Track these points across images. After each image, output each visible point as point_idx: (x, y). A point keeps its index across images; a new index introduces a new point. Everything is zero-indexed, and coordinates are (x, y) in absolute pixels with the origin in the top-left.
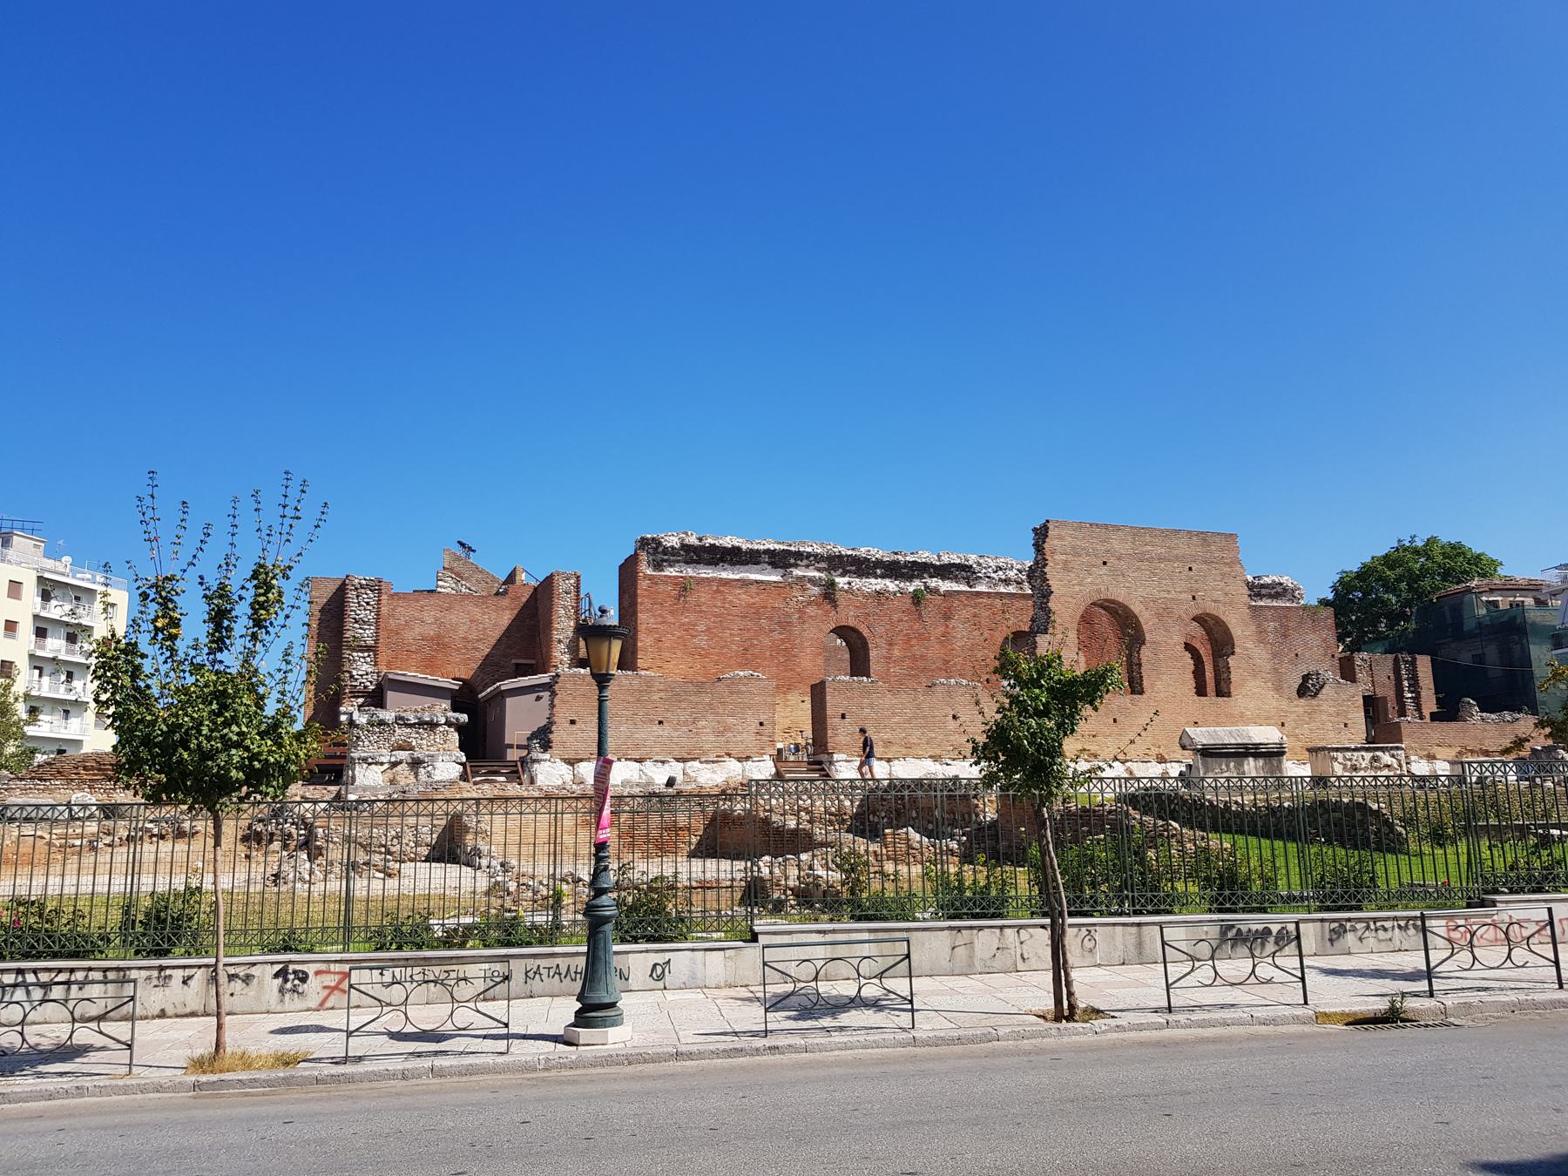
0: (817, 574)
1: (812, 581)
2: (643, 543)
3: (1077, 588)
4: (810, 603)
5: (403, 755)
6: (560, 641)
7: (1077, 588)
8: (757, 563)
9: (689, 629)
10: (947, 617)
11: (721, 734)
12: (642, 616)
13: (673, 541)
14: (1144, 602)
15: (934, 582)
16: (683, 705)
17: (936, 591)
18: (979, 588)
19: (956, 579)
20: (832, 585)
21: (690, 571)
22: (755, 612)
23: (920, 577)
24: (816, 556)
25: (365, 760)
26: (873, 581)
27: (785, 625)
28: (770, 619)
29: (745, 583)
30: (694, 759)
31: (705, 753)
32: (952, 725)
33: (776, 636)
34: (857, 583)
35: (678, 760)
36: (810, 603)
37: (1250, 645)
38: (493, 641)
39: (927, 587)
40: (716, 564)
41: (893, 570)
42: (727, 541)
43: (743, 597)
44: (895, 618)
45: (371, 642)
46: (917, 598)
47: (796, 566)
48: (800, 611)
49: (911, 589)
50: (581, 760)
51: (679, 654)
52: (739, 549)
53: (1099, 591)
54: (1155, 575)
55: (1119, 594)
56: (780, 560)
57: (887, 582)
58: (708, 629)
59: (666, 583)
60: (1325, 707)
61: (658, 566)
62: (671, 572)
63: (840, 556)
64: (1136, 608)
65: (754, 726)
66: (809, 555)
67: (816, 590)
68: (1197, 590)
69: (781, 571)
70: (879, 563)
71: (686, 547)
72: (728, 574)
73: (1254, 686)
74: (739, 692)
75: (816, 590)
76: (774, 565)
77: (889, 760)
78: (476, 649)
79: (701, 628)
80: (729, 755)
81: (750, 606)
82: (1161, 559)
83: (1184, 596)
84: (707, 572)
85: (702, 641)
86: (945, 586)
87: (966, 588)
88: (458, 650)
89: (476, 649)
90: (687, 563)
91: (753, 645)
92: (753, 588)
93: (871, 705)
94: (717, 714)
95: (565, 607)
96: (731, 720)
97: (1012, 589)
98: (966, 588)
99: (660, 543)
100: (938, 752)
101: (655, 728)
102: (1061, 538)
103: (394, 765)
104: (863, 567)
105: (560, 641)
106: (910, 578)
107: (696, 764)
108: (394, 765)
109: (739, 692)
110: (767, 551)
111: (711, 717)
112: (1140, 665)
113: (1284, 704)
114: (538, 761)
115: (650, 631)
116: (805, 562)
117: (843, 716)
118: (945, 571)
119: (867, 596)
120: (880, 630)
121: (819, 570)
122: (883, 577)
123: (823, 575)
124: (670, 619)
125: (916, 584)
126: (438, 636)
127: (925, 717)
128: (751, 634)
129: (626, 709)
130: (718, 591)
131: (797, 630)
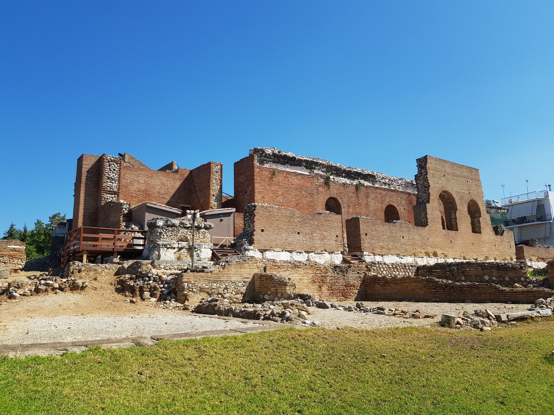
0: (321, 173)
1: (321, 176)
2: (256, 151)
4: (320, 186)
5: (184, 244)
6: (214, 195)
8: (300, 166)
9: (275, 192)
10: (367, 197)
11: (322, 240)
12: (256, 185)
13: (269, 151)
15: (362, 181)
16: (307, 225)
17: (363, 185)
18: (377, 186)
19: (369, 181)
20: (328, 178)
21: (274, 166)
22: (300, 188)
23: (358, 179)
24: (323, 165)
25: (165, 246)
26: (341, 178)
27: (311, 195)
28: (306, 191)
29: (297, 174)
30: (312, 252)
31: (316, 249)
33: (308, 199)
34: (337, 179)
35: (305, 252)
36: (320, 186)
37: (485, 213)
38: (172, 195)
39: (360, 183)
40: (285, 165)
41: (350, 175)
42: (290, 154)
43: (295, 181)
44: (350, 195)
45: (116, 190)
46: (357, 187)
47: (315, 169)
48: (317, 189)
49: (355, 184)
50: (266, 250)
52: (295, 158)
53: (443, 187)
56: (310, 165)
57: (346, 179)
58: (283, 194)
59: (266, 170)
61: (262, 162)
62: (267, 166)
63: (332, 166)
64: (454, 196)
65: (334, 238)
66: (321, 164)
67: (322, 180)
69: (309, 170)
70: (344, 171)
71: (274, 155)
72: (289, 169)
74: (328, 220)
75: (322, 180)
76: (307, 167)
77: (382, 256)
78: (164, 198)
79: (280, 193)
80: (325, 250)
81: (298, 185)
82: (460, 176)
84: (281, 168)
86: (366, 183)
87: (371, 185)
88: (156, 198)
89: (164, 198)
90: (273, 162)
92: (300, 177)
93: (376, 230)
95: (216, 179)
96: (325, 234)
97: (387, 187)
98: (371, 185)
99: (264, 152)
100: (399, 252)
101: (297, 235)
102: (431, 164)
103: (180, 249)
104: (338, 172)
105: (214, 195)
106: (354, 179)
107: (313, 254)
108: (180, 249)
109: (328, 220)
110: (305, 161)
111: (318, 232)
112: (456, 219)
114: (248, 250)
115: (260, 193)
116: (318, 167)
117: (366, 234)
118: (366, 177)
119: (340, 185)
120: (345, 200)
121: (322, 171)
122: (345, 177)
123: (325, 174)
125: (355, 182)
126: (146, 190)
128: (299, 198)
129: (284, 225)
130: (286, 177)
131: (316, 197)
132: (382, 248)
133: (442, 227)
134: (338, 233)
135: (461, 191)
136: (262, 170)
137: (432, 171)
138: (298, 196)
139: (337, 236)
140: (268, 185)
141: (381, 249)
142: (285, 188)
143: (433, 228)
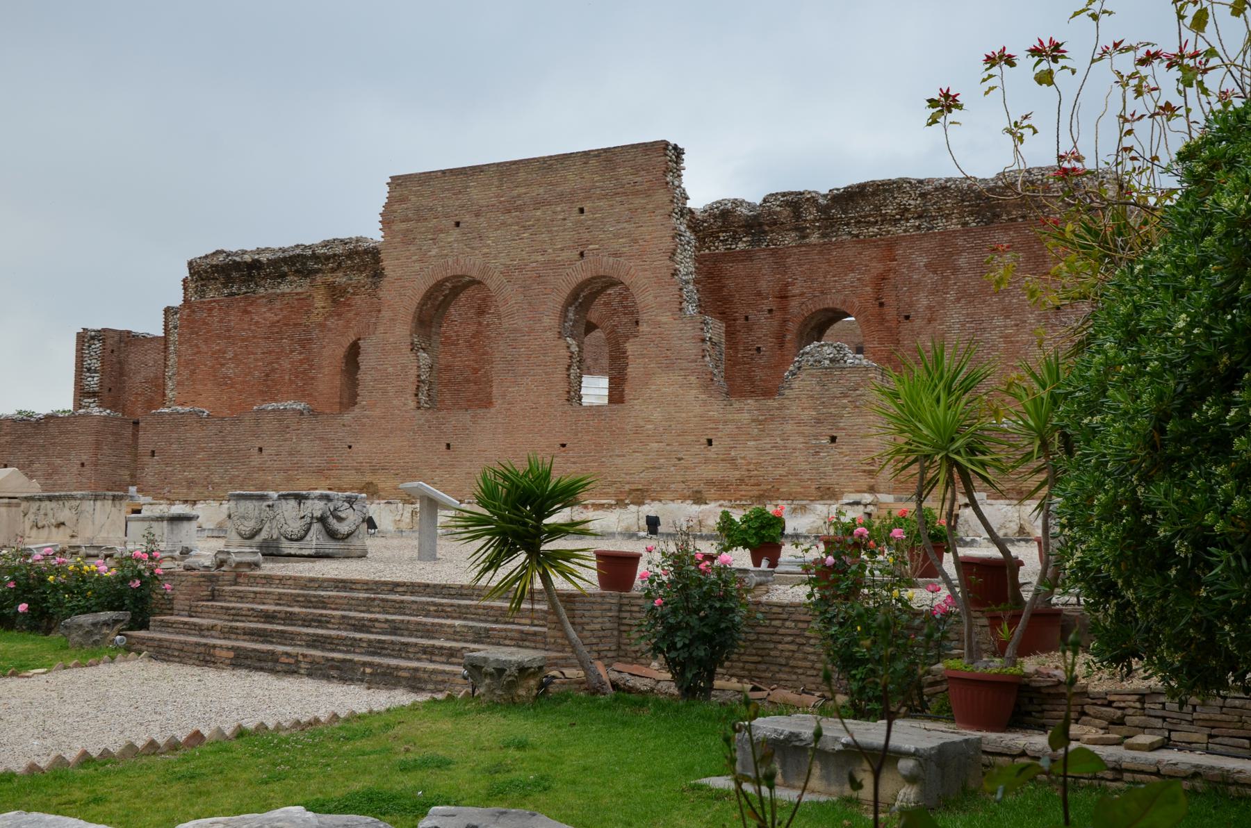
3: (417, 266)
7: (417, 266)
14: (507, 272)
16: (23, 448)
27: (305, 343)
28: (291, 338)
32: (256, 460)
51: (209, 385)
54: (525, 228)
55: (470, 263)
60: (794, 410)
65: (76, 469)
68: (589, 242)
73: (665, 384)
79: (230, 355)
81: (273, 324)
82: (539, 203)
83: (566, 255)
85: (230, 370)
91: (273, 370)
94: (47, 455)
96: (59, 461)
111: (43, 459)
113: (716, 409)
124: (204, 348)
127: (229, 452)
130: (246, 312)
132: (191, 483)
133: (412, 404)
134: (84, 458)
135: (533, 258)
136: (194, 312)
137: (404, 226)
138: (270, 353)
139: (83, 465)
140: (206, 341)
141: (189, 488)
142: (243, 340)
143: (377, 412)
